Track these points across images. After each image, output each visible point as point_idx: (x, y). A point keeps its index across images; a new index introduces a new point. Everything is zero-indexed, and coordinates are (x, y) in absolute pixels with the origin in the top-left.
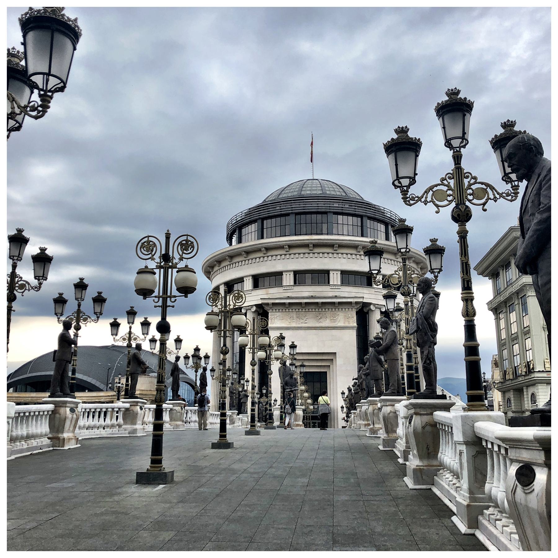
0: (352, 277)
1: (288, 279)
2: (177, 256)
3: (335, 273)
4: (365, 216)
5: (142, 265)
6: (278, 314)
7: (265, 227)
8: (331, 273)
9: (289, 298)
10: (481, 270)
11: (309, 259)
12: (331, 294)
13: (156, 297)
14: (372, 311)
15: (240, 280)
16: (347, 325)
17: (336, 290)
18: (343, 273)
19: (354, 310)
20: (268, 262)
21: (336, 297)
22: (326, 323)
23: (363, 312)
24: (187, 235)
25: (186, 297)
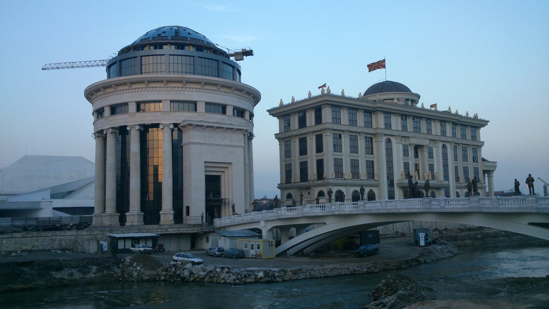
6: (197, 133)
10: (274, 112)
16: (239, 144)
18: (235, 108)
20: (186, 92)
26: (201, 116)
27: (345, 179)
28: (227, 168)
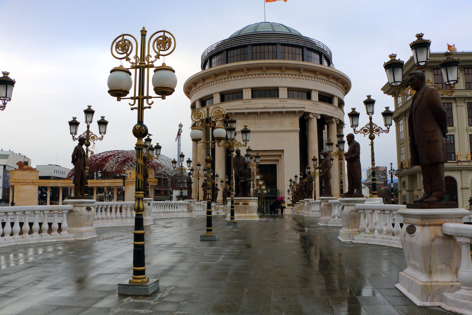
0: (296, 93)
1: (247, 94)
2: (153, 54)
3: (283, 89)
4: (305, 47)
5: (117, 64)
7: (229, 56)
8: (280, 89)
9: (247, 108)
11: (263, 79)
12: (280, 106)
13: (132, 98)
14: (311, 118)
15: (211, 97)
17: (284, 102)
18: (290, 90)
19: (297, 117)
20: (232, 82)
21: (284, 108)
22: (276, 127)
23: (304, 120)
24: (164, 32)
25: (163, 98)
26: (248, 103)
27: (458, 162)
28: (280, 156)
